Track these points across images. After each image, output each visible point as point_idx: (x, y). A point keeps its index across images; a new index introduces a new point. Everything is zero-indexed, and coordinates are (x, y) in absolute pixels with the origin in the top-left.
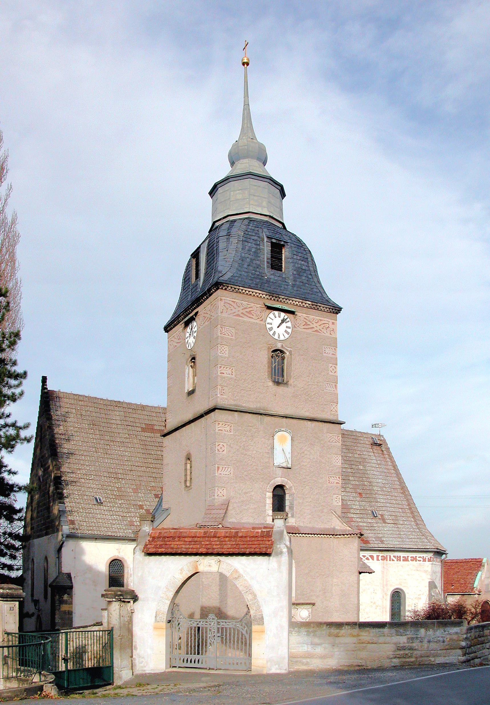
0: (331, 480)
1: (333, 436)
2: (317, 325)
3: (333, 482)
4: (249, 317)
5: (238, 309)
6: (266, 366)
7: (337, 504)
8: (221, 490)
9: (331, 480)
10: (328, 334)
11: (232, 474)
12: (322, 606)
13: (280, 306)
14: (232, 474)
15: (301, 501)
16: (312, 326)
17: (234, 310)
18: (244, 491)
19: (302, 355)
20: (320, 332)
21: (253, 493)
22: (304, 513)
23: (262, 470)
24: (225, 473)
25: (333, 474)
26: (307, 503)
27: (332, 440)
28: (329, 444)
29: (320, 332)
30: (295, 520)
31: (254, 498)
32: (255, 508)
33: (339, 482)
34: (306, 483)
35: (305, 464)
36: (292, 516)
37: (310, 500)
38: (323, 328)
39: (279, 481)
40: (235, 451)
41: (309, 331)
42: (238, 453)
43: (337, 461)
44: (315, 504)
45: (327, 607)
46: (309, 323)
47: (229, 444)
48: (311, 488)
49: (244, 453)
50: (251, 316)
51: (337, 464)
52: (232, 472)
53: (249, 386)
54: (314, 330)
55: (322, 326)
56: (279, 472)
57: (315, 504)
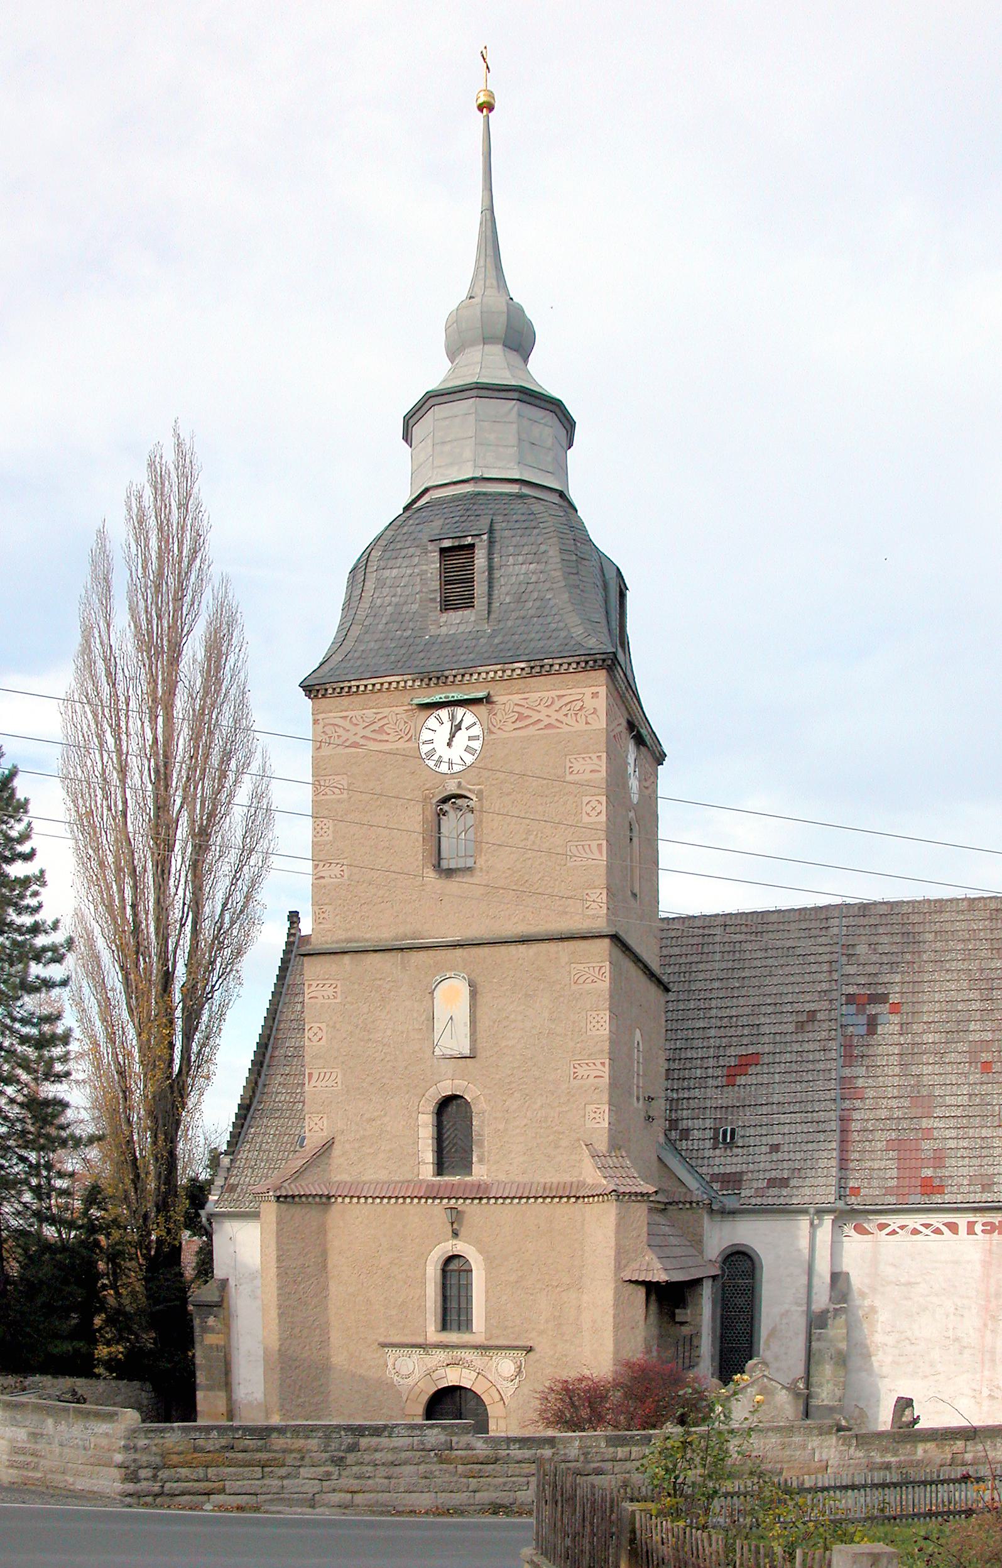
0: (581, 1071)
1: (587, 969)
2: (550, 711)
3: (585, 1077)
4: (380, 741)
5: (353, 729)
6: (417, 841)
7: (597, 1126)
8: (316, 1120)
9: (581, 1071)
10: (582, 726)
11: (339, 1083)
12: (552, 1353)
13: (443, 696)
14: (339, 1083)
15: (501, 1127)
16: (536, 717)
17: (345, 735)
18: (367, 1116)
19: (509, 794)
20: (558, 725)
21: (387, 1119)
22: (510, 1152)
23: (406, 1068)
24: (324, 1083)
25: (586, 1057)
26: (518, 1131)
27: (585, 977)
28: (574, 987)
29: (558, 725)
30: (488, 1170)
31: (389, 1129)
32: (391, 1151)
33: (602, 1074)
34: (514, 1085)
35: (510, 1043)
36: (481, 1161)
37: (525, 1121)
38: (566, 715)
39: (446, 1089)
40: (344, 1036)
41: (532, 730)
42: (352, 1039)
43: (598, 1026)
44: (538, 1130)
45: (566, 1356)
46: (527, 712)
47: (331, 1023)
48: (527, 1095)
49: (366, 1038)
50: (385, 737)
51: (598, 1033)
52: (339, 1080)
53: (381, 893)
54: (541, 725)
55: (564, 710)
56: (448, 1067)
57: (538, 1130)
